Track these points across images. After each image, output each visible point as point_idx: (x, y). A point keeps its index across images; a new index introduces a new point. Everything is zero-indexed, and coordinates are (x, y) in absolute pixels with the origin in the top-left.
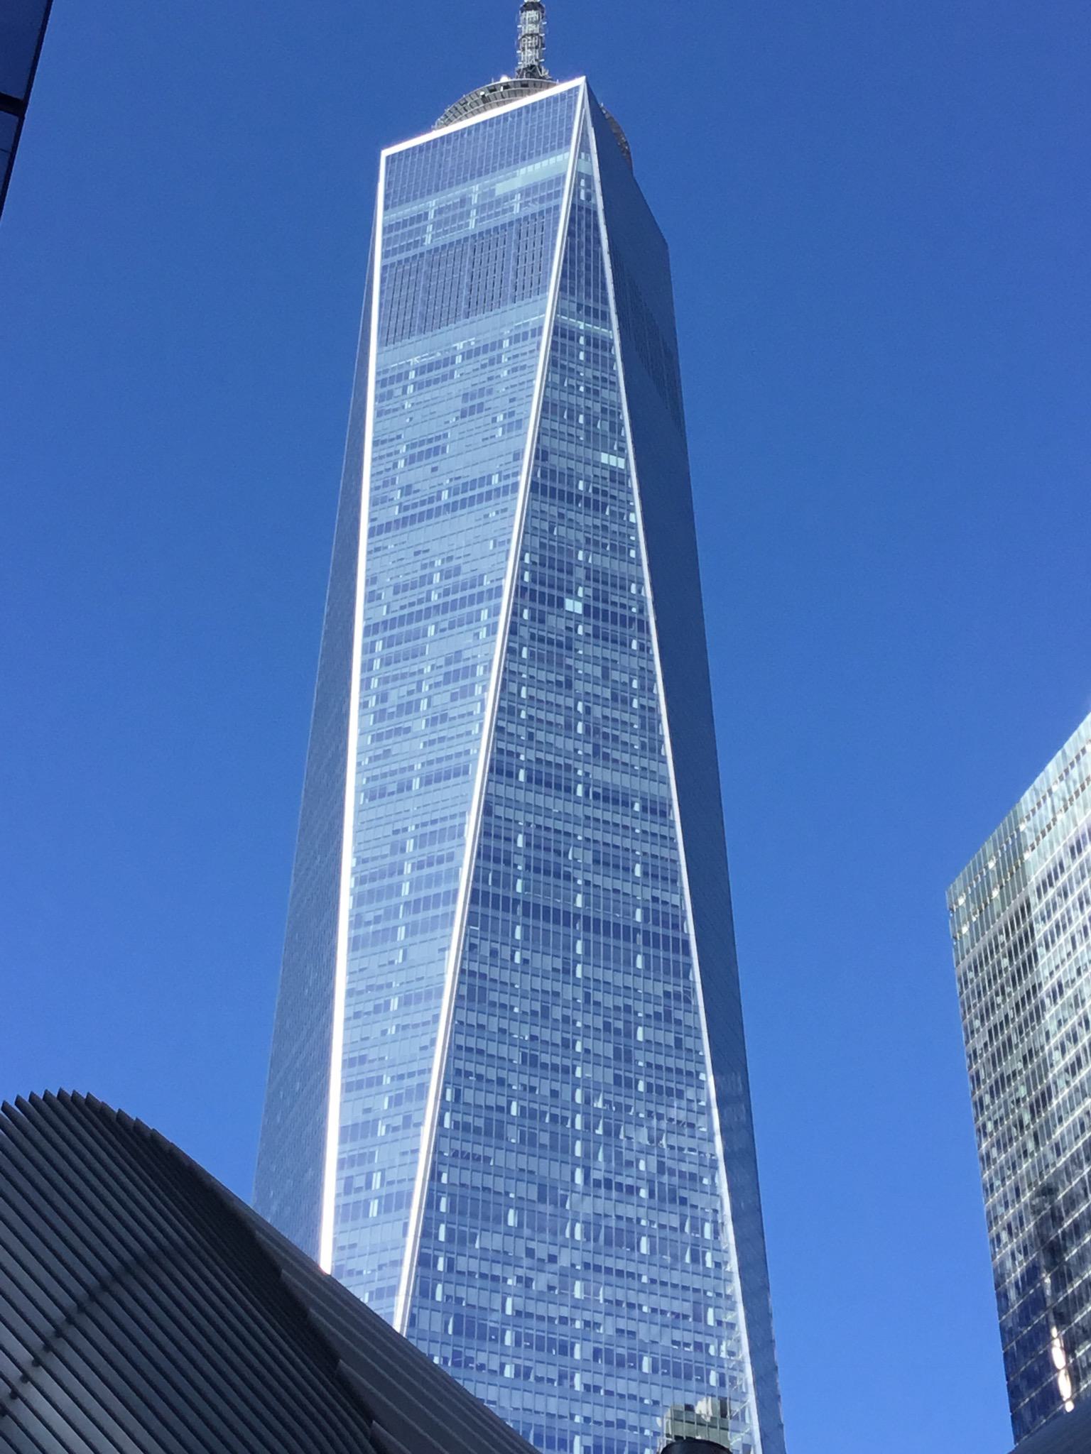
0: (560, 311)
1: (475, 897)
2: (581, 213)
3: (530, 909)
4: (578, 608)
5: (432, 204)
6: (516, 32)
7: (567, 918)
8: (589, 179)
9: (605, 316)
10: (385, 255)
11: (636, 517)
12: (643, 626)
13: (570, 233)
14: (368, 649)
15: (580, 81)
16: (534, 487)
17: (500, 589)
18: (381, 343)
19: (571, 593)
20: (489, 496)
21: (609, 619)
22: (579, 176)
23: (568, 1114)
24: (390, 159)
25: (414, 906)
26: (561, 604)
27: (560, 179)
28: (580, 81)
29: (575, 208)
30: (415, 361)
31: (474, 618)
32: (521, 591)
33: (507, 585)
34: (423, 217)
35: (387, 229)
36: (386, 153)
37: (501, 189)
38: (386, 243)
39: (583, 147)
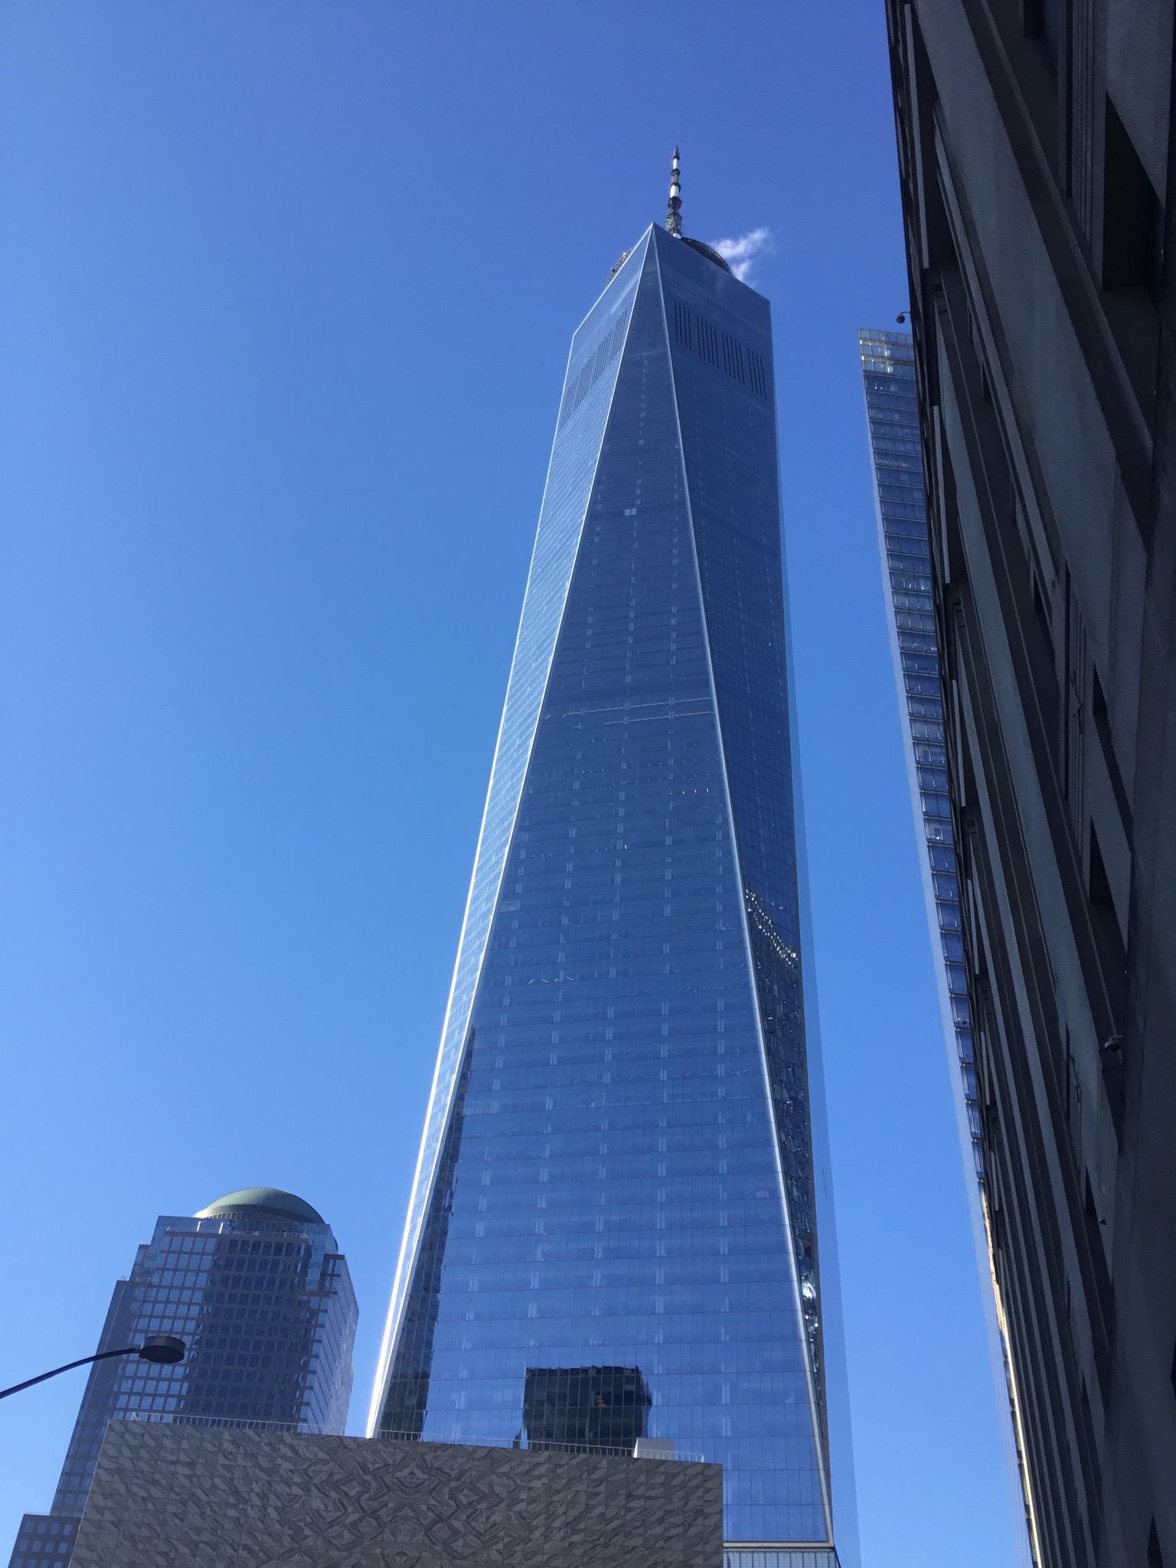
2: (646, 293)
4: (634, 511)
26: (623, 512)
37: (614, 309)
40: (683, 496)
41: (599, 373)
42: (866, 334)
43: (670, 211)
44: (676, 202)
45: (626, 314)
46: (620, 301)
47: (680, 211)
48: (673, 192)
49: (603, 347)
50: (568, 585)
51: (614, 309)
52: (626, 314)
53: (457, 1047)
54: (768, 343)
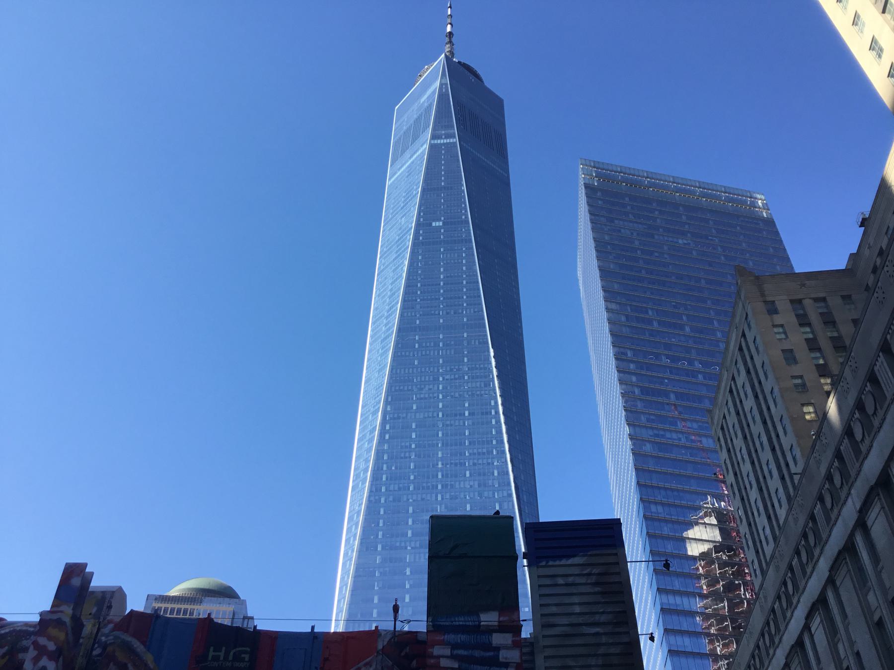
0: (434, 129)
2: (442, 97)
4: (441, 224)
5: (405, 118)
11: (464, 188)
13: (438, 102)
14: (381, 262)
16: (423, 190)
22: (441, 85)
23: (435, 395)
37: (422, 100)
40: (467, 217)
41: (416, 137)
42: (584, 162)
43: (447, 39)
44: (451, 34)
45: (430, 106)
46: (426, 97)
47: (453, 40)
48: (449, 28)
49: (417, 121)
50: (406, 263)
51: (422, 100)
52: (430, 106)
53: (357, 524)
54: (503, 124)
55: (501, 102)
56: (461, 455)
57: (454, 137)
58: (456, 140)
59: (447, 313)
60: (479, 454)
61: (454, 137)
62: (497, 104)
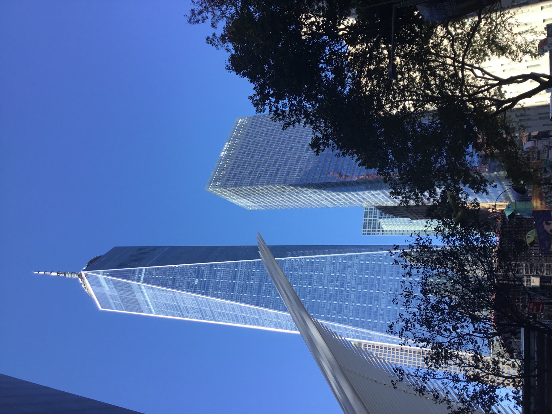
0: (134, 280)
1: (257, 305)
2: (112, 274)
3: (259, 293)
4: (197, 280)
5: (111, 301)
6: (71, 278)
7: (260, 285)
8: (104, 272)
9: (134, 270)
10: (123, 310)
11: (177, 266)
12: (199, 266)
13: (116, 277)
14: (208, 319)
15: (83, 273)
17: (195, 297)
18: (143, 312)
19: (194, 281)
20: (175, 296)
21: (198, 273)
22: (103, 274)
24: (102, 308)
25: (260, 316)
27: (105, 278)
28: (83, 273)
29: (111, 275)
30: (146, 307)
31: (200, 300)
32: (195, 292)
33: (193, 295)
34: (114, 303)
35: (118, 310)
36: (100, 308)
38: (120, 310)
39: (97, 273)
45: (115, 283)
52: (115, 283)
55: (115, 248)
56: (333, 278)
57: (142, 269)
58: (144, 268)
59: (252, 279)
60: (334, 269)
61: (142, 269)
62: (117, 251)
